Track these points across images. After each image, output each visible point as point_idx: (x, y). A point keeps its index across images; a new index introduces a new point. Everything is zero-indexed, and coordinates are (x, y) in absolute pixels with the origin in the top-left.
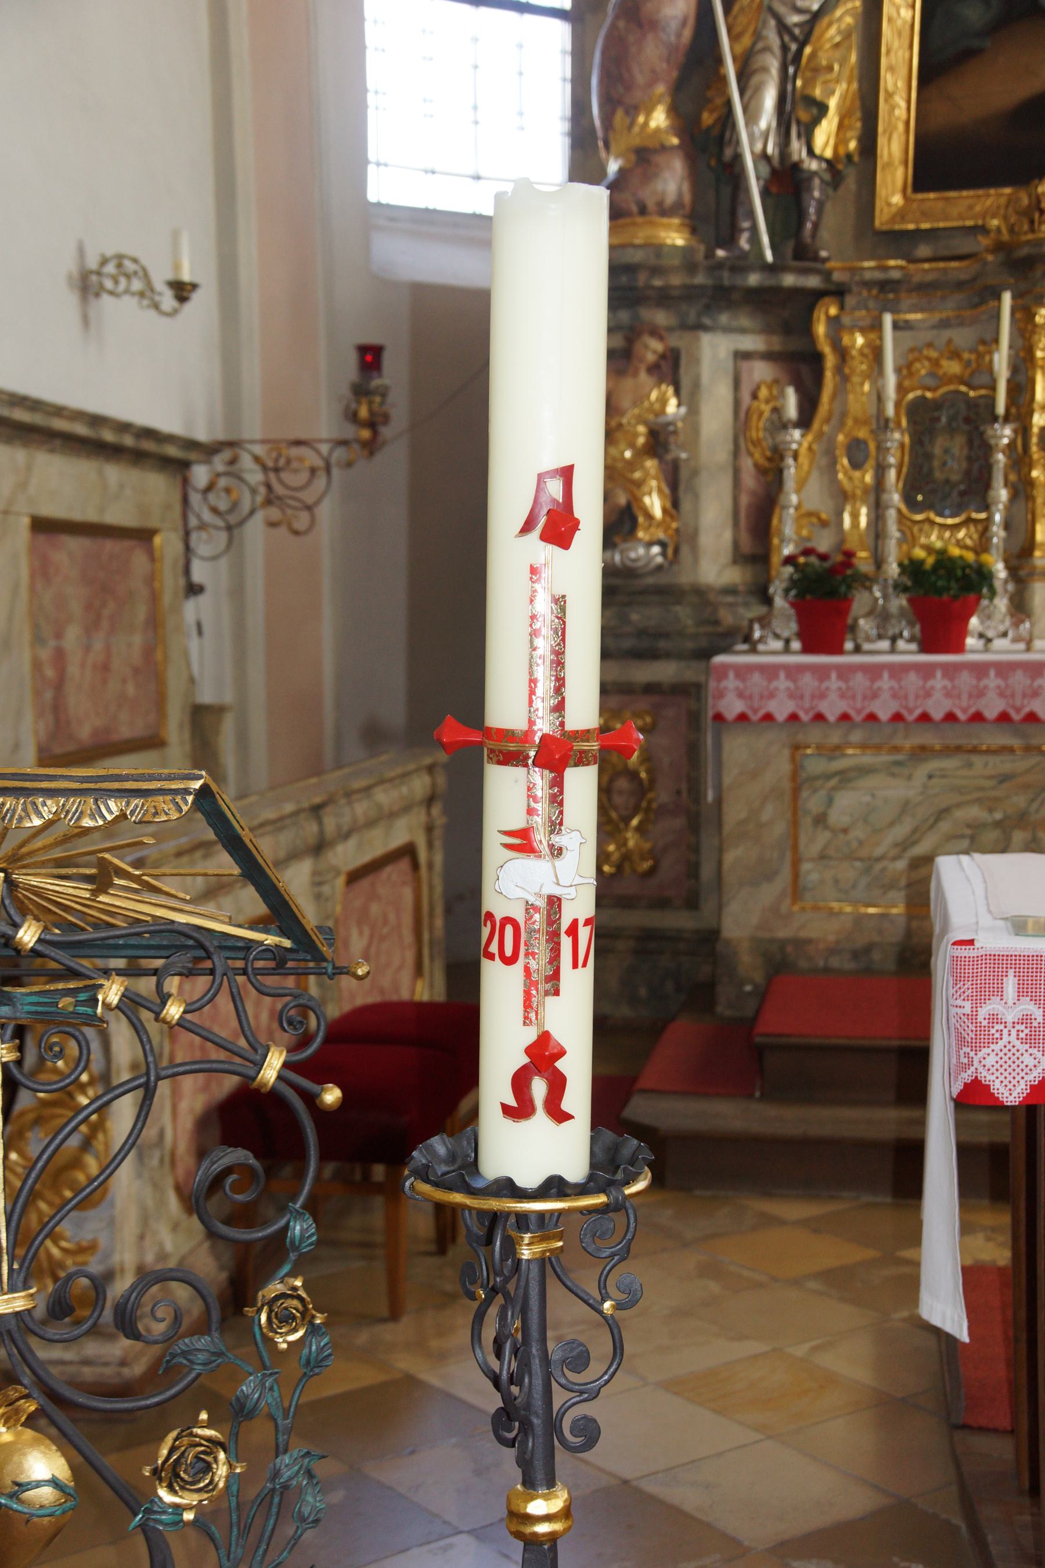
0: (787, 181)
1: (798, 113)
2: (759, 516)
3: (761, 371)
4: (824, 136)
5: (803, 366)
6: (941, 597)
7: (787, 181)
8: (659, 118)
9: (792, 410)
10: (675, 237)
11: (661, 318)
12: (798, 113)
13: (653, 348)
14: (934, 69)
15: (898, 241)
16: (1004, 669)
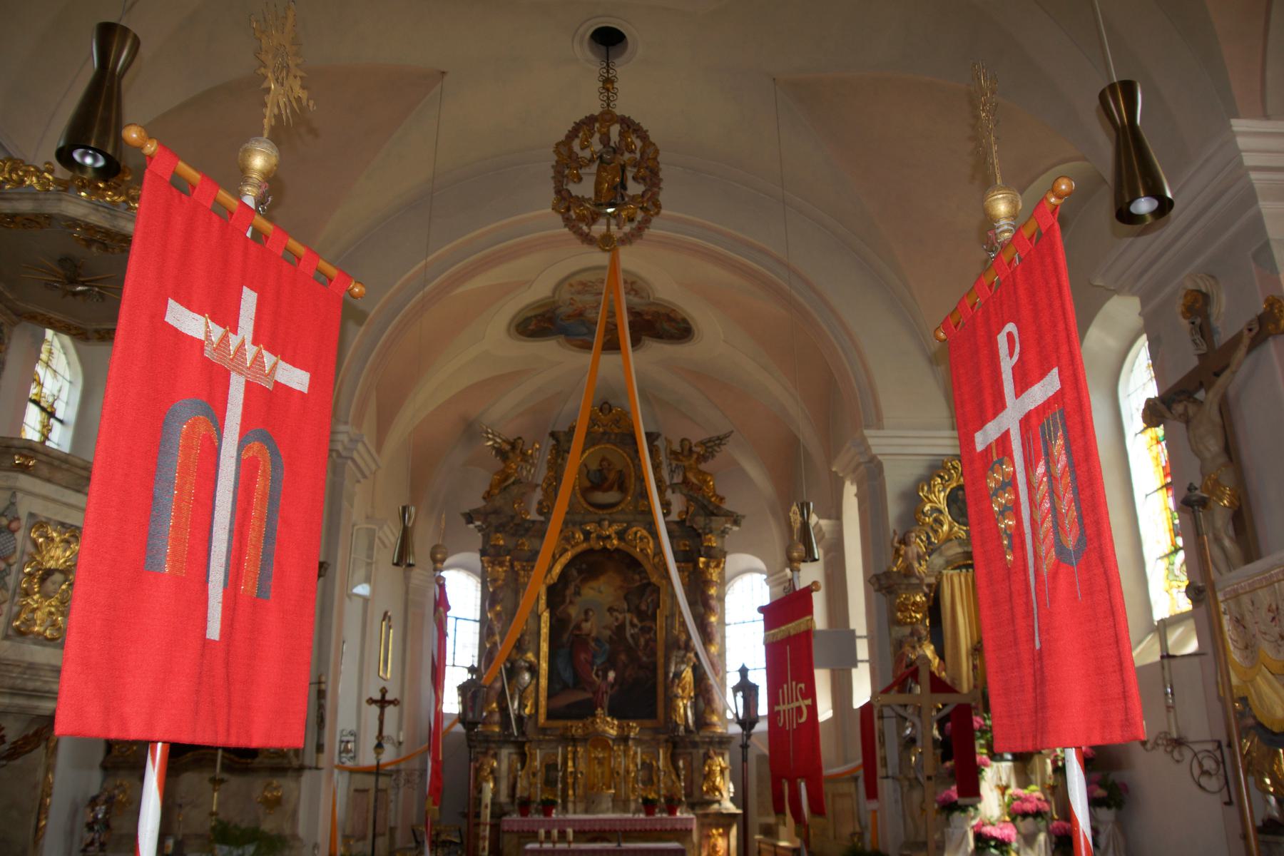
0: (520, 718)
1: (522, 706)
2: (513, 788)
3: (514, 757)
4: (527, 711)
5: (523, 757)
6: (547, 807)
7: (520, 718)
8: (494, 705)
9: (519, 766)
10: (497, 729)
11: (493, 745)
12: (522, 706)
13: (492, 752)
14: (550, 696)
15: (543, 730)
16: (559, 821)
